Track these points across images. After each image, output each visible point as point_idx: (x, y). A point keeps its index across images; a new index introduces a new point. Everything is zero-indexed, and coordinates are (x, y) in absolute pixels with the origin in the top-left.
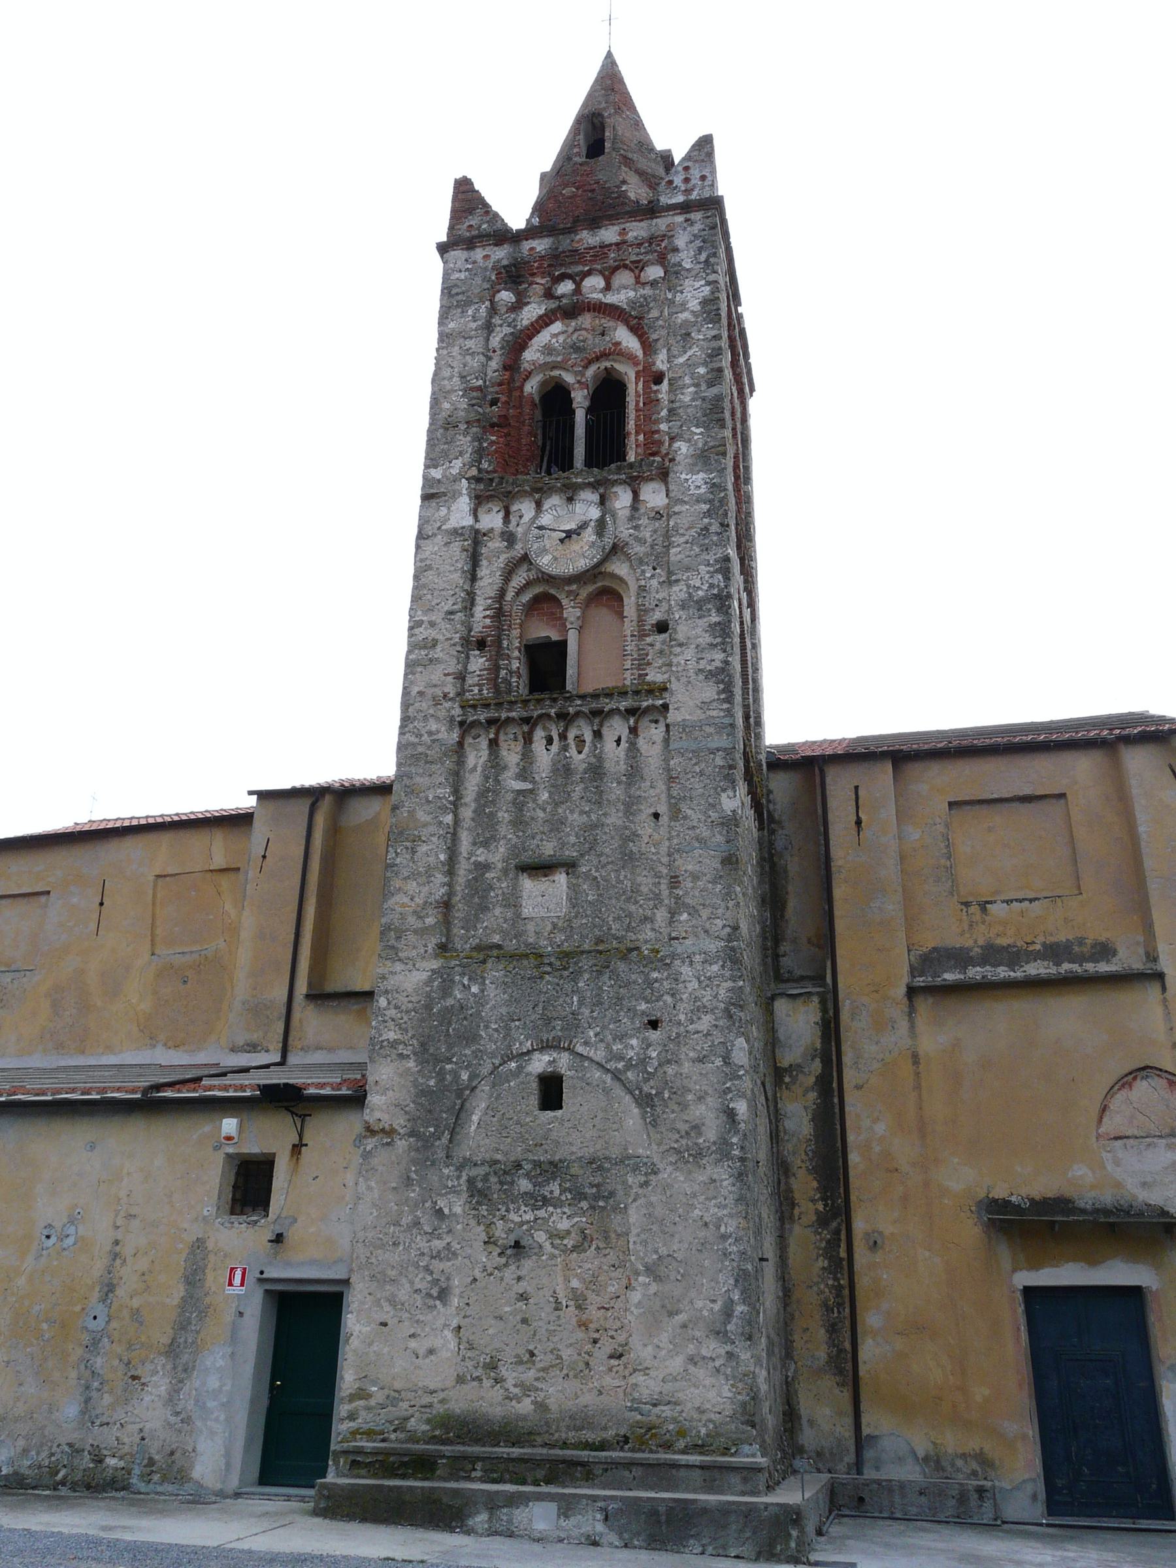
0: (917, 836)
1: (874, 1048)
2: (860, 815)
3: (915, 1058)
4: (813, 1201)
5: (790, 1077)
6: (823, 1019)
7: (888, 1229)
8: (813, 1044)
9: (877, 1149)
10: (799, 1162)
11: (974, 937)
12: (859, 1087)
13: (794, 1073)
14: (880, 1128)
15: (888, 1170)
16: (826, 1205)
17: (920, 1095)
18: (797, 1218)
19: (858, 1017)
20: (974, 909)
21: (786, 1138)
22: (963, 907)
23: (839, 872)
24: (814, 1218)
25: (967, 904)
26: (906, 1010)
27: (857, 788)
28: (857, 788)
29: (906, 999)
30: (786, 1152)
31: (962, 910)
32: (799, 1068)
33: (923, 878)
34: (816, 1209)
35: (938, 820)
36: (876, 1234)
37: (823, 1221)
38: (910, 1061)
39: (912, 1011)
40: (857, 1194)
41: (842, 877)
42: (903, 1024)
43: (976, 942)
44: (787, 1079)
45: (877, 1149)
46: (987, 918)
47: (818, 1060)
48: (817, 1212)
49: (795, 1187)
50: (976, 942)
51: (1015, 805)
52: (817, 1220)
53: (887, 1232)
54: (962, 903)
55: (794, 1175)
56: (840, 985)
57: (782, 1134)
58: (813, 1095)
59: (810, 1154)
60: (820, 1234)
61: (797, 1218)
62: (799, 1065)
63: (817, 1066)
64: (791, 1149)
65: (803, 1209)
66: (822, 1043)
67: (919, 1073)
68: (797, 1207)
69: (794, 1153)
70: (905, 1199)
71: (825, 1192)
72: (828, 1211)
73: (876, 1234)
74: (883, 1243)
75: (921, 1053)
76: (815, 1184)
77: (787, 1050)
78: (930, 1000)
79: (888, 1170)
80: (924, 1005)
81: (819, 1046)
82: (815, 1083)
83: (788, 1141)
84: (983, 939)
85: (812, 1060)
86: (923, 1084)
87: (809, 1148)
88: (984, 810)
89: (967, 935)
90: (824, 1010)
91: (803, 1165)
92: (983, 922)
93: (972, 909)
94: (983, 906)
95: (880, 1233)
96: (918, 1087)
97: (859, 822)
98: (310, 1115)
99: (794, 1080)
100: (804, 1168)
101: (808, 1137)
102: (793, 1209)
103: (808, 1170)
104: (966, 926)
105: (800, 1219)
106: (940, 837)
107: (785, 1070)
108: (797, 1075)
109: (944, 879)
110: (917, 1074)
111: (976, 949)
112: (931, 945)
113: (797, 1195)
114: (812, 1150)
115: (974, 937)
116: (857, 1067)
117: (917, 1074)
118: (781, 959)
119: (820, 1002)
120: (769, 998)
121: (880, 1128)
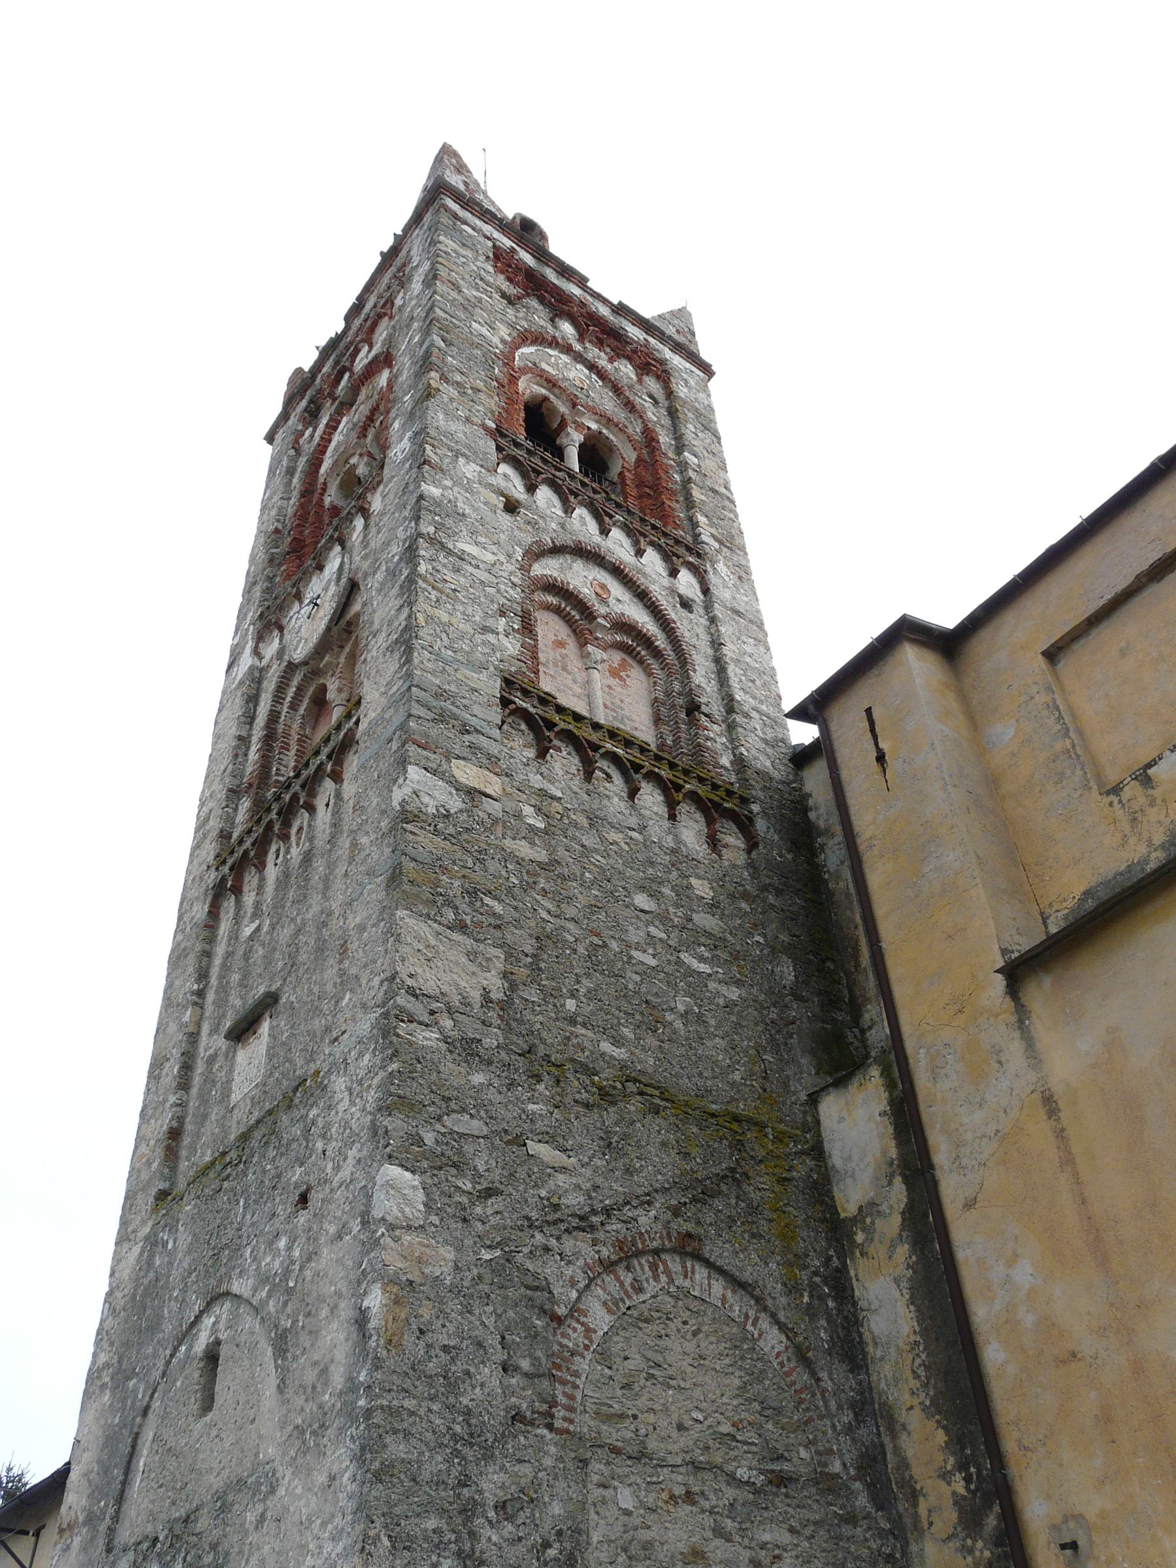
0: (1011, 731)
1: (978, 1116)
2: (881, 746)
3: (1050, 1104)
4: (945, 1476)
5: (863, 1230)
6: (891, 1102)
7: (1091, 1504)
8: (884, 1153)
9: (1028, 1320)
10: (907, 1396)
11: (1145, 835)
12: (970, 1204)
13: (868, 1221)
14: (1024, 1274)
15: (1061, 1362)
16: (968, 1480)
17: (1075, 1174)
18: (925, 1525)
19: (942, 1072)
20: (1132, 790)
21: (879, 1353)
22: (1112, 797)
23: (871, 847)
24: (954, 1516)
25: (1116, 790)
26: (1013, 1019)
27: (869, 711)
28: (869, 711)
29: (1008, 999)
30: (883, 1385)
31: (1111, 804)
32: (869, 1209)
33: (1038, 789)
34: (954, 1493)
35: (1035, 689)
36: (1072, 1524)
37: (970, 1519)
38: (1042, 1112)
39: (1021, 1011)
40: (1016, 1434)
41: (876, 852)
42: (1015, 1049)
43: (1150, 843)
44: (860, 1238)
45: (1028, 1320)
46: (1156, 793)
47: (898, 1179)
48: (958, 1501)
49: (910, 1453)
50: (1150, 843)
51: (1155, 589)
52: (960, 1518)
53: (1091, 1514)
54: (1108, 793)
55: (904, 1427)
56: (906, 1029)
57: (870, 1349)
58: (903, 1250)
59: (922, 1372)
60: (971, 1551)
61: (925, 1525)
62: (873, 1204)
63: (898, 1193)
64: (890, 1375)
65: (932, 1500)
66: (898, 1145)
67: (1063, 1130)
68: (921, 1499)
69: (896, 1381)
70: (1106, 1418)
71: (963, 1449)
72: (974, 1493)
73: (1072, 1524)
74: (1091, 1542)
75: (1058, 1089)
76: (941, 1437)
77: (849, 1181)
78: (1047, 981)
79: (1061, 1362)
80: (1039, 993)
81: (893, 1153)
82: (903, 1227)
83: (882, 1359)
84: (1162, 830)
85: (890, 1183)
86: (1076, 1149)
87: (918, 1362)
88: (1105, 633)
89: (1132, 840)
90: (890, 1085)
91: (916, 1401)
92: (1152, 804)
93: (1127, 793)
94: (1143, 777)
95: (1079, 1518)
96: (1068, 1160)
97: (881, 758)
98: (43, 1527)
99: (869, 1231)
100: (918, 1409)
101: (912, 1338)
102: (915, 1505)
103: (925, 1409)
104: (1125, 826)
105: (931, 1524)
106: (1045, 713)
107: (854, 1220)
108: (873, 1223)
109: (1068, 772)
110: (1060, 1134)
111: (1154, 855)
112: (1078, 891)
113: (917, 1471)
114: (923, 1364)
115: (1145, 835)
116: (960, 1167)
117: (1060, 1134)
118: (868, 1034)
119: (882, 1075)
120: (806, 1103)
121: (1024, 1274)
